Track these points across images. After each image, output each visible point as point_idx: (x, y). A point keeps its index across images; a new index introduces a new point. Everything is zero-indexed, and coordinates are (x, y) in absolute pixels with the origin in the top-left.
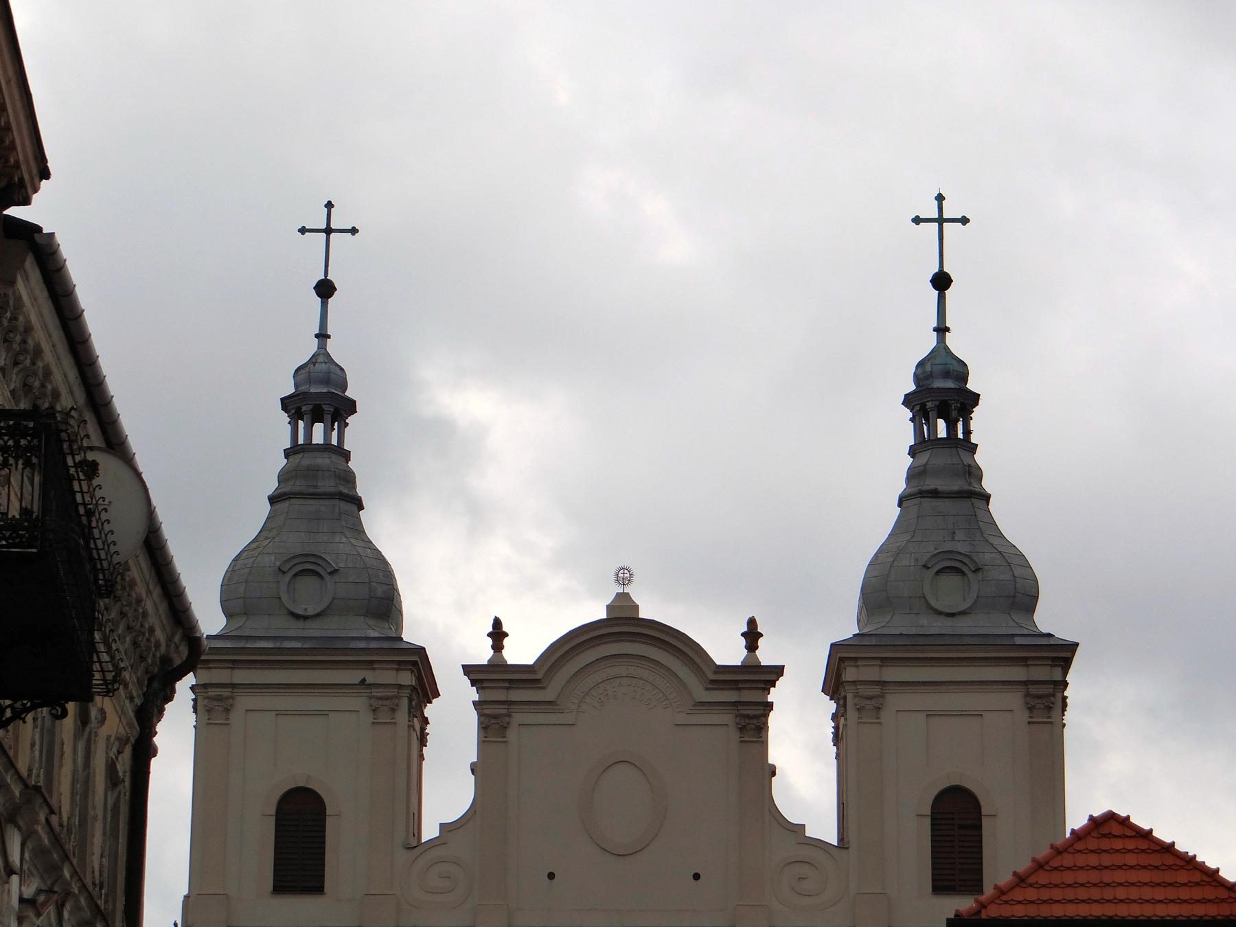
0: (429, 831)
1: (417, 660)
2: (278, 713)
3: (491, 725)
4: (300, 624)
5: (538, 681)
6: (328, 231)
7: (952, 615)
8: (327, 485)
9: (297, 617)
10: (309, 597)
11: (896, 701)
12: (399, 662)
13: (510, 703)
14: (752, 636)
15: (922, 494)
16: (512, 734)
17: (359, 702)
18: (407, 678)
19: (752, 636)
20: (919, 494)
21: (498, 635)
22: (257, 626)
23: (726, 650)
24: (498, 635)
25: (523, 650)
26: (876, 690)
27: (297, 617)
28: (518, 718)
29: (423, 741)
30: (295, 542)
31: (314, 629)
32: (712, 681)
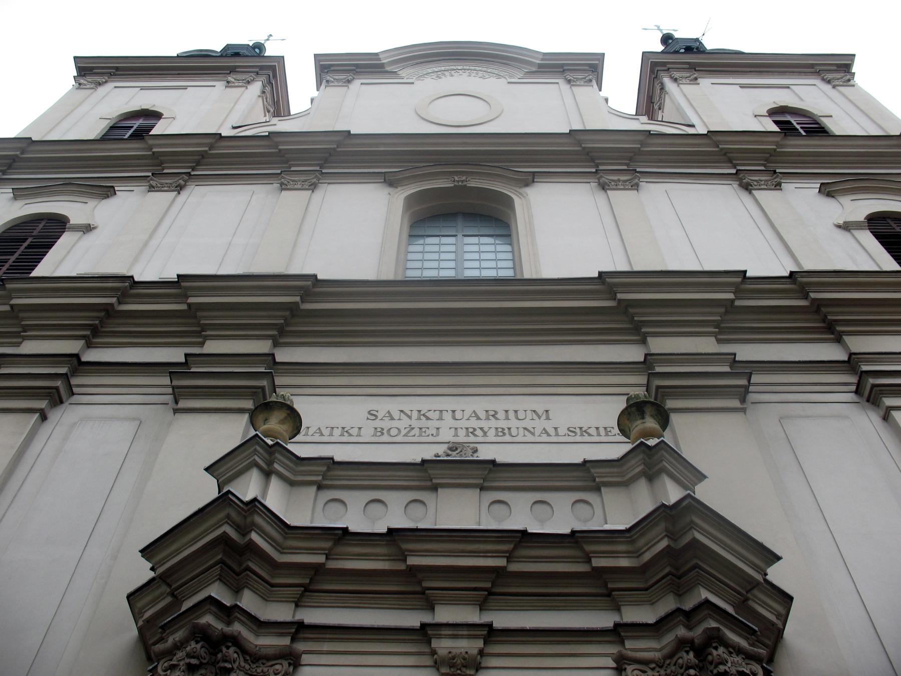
16: (351, 86)
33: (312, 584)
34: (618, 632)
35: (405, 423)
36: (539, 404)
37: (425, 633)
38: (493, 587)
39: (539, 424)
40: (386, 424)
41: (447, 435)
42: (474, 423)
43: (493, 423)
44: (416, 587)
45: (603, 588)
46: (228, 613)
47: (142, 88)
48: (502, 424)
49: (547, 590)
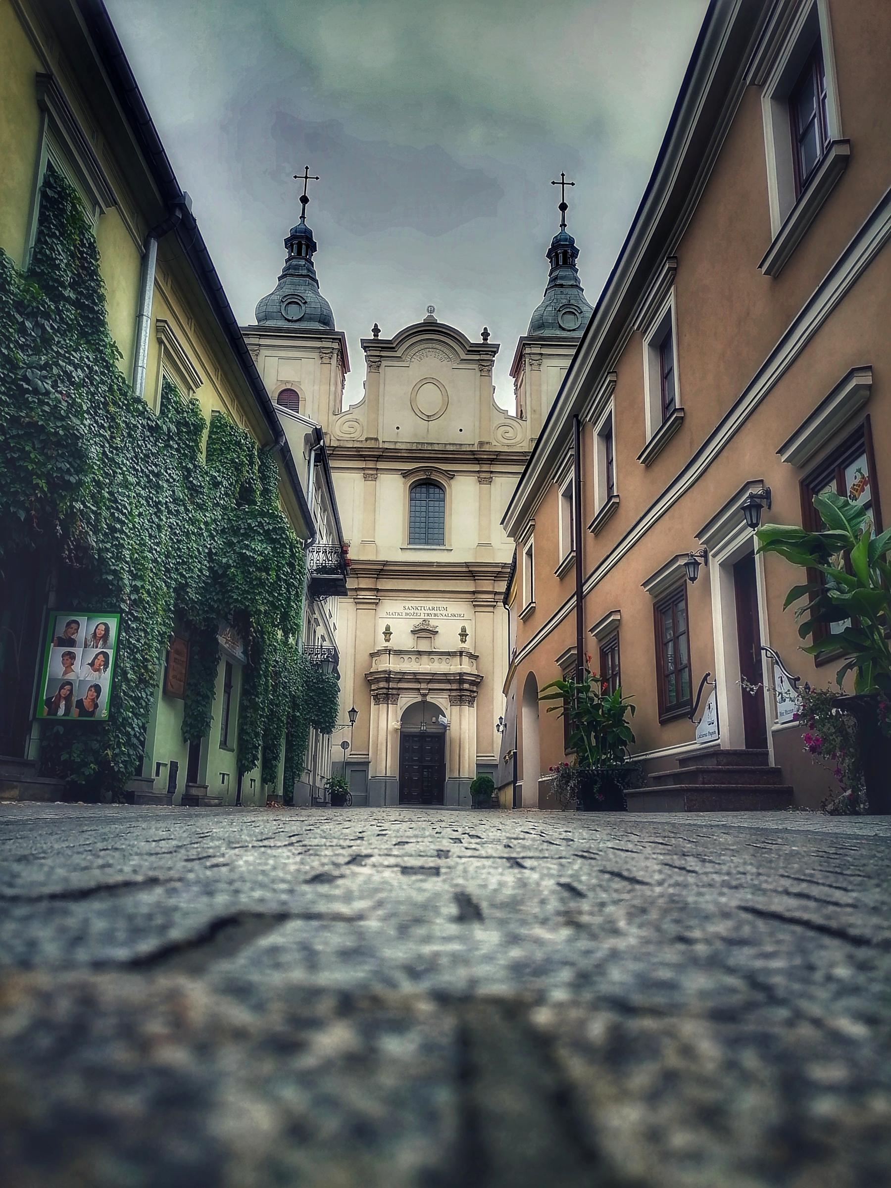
0: (345, 408)
1: (340, 340)
2: (280, 358)
3: (374, 364)
4: (290, 323)
5: (394, 348)
6: (306, 178)
7: (570, 331)
8: (305, 272)
9: (289, 321)
10: (294, 312)
11: (546, 362)
12: (333, 339)
13: (381, 356)
14: (485, 335)
15: (556, 285)
17: (316, 355)
18: (336, 345)
19: (485, 335)
20: (555, 284)
21: (376, 330)
22: (269, 323)
23: (475, 338)
24: (376, 330)
25: (387, 335)
26: (539, 357)
27: (289, 321)
28: (384, 363)
29: (343, 385)
30: (287, 290)
31: (296, 326)
32: (469, 351)
33: (400, 680)
34: (450, 690)
35: (412, 611)
36: (445, 604)
37: (419, 689)
38: (430, 681)
39: (444, 612)
40: (408, 611)
41: (422, 616)
42: (429, 612)
43: (433, 612)
44: (418, 681)
45: (449, 682)
46: (388, 689)
47: (280, 358)
48: (436, 612)
49: (440, 681)
